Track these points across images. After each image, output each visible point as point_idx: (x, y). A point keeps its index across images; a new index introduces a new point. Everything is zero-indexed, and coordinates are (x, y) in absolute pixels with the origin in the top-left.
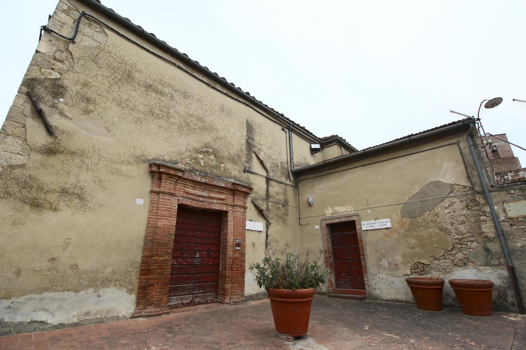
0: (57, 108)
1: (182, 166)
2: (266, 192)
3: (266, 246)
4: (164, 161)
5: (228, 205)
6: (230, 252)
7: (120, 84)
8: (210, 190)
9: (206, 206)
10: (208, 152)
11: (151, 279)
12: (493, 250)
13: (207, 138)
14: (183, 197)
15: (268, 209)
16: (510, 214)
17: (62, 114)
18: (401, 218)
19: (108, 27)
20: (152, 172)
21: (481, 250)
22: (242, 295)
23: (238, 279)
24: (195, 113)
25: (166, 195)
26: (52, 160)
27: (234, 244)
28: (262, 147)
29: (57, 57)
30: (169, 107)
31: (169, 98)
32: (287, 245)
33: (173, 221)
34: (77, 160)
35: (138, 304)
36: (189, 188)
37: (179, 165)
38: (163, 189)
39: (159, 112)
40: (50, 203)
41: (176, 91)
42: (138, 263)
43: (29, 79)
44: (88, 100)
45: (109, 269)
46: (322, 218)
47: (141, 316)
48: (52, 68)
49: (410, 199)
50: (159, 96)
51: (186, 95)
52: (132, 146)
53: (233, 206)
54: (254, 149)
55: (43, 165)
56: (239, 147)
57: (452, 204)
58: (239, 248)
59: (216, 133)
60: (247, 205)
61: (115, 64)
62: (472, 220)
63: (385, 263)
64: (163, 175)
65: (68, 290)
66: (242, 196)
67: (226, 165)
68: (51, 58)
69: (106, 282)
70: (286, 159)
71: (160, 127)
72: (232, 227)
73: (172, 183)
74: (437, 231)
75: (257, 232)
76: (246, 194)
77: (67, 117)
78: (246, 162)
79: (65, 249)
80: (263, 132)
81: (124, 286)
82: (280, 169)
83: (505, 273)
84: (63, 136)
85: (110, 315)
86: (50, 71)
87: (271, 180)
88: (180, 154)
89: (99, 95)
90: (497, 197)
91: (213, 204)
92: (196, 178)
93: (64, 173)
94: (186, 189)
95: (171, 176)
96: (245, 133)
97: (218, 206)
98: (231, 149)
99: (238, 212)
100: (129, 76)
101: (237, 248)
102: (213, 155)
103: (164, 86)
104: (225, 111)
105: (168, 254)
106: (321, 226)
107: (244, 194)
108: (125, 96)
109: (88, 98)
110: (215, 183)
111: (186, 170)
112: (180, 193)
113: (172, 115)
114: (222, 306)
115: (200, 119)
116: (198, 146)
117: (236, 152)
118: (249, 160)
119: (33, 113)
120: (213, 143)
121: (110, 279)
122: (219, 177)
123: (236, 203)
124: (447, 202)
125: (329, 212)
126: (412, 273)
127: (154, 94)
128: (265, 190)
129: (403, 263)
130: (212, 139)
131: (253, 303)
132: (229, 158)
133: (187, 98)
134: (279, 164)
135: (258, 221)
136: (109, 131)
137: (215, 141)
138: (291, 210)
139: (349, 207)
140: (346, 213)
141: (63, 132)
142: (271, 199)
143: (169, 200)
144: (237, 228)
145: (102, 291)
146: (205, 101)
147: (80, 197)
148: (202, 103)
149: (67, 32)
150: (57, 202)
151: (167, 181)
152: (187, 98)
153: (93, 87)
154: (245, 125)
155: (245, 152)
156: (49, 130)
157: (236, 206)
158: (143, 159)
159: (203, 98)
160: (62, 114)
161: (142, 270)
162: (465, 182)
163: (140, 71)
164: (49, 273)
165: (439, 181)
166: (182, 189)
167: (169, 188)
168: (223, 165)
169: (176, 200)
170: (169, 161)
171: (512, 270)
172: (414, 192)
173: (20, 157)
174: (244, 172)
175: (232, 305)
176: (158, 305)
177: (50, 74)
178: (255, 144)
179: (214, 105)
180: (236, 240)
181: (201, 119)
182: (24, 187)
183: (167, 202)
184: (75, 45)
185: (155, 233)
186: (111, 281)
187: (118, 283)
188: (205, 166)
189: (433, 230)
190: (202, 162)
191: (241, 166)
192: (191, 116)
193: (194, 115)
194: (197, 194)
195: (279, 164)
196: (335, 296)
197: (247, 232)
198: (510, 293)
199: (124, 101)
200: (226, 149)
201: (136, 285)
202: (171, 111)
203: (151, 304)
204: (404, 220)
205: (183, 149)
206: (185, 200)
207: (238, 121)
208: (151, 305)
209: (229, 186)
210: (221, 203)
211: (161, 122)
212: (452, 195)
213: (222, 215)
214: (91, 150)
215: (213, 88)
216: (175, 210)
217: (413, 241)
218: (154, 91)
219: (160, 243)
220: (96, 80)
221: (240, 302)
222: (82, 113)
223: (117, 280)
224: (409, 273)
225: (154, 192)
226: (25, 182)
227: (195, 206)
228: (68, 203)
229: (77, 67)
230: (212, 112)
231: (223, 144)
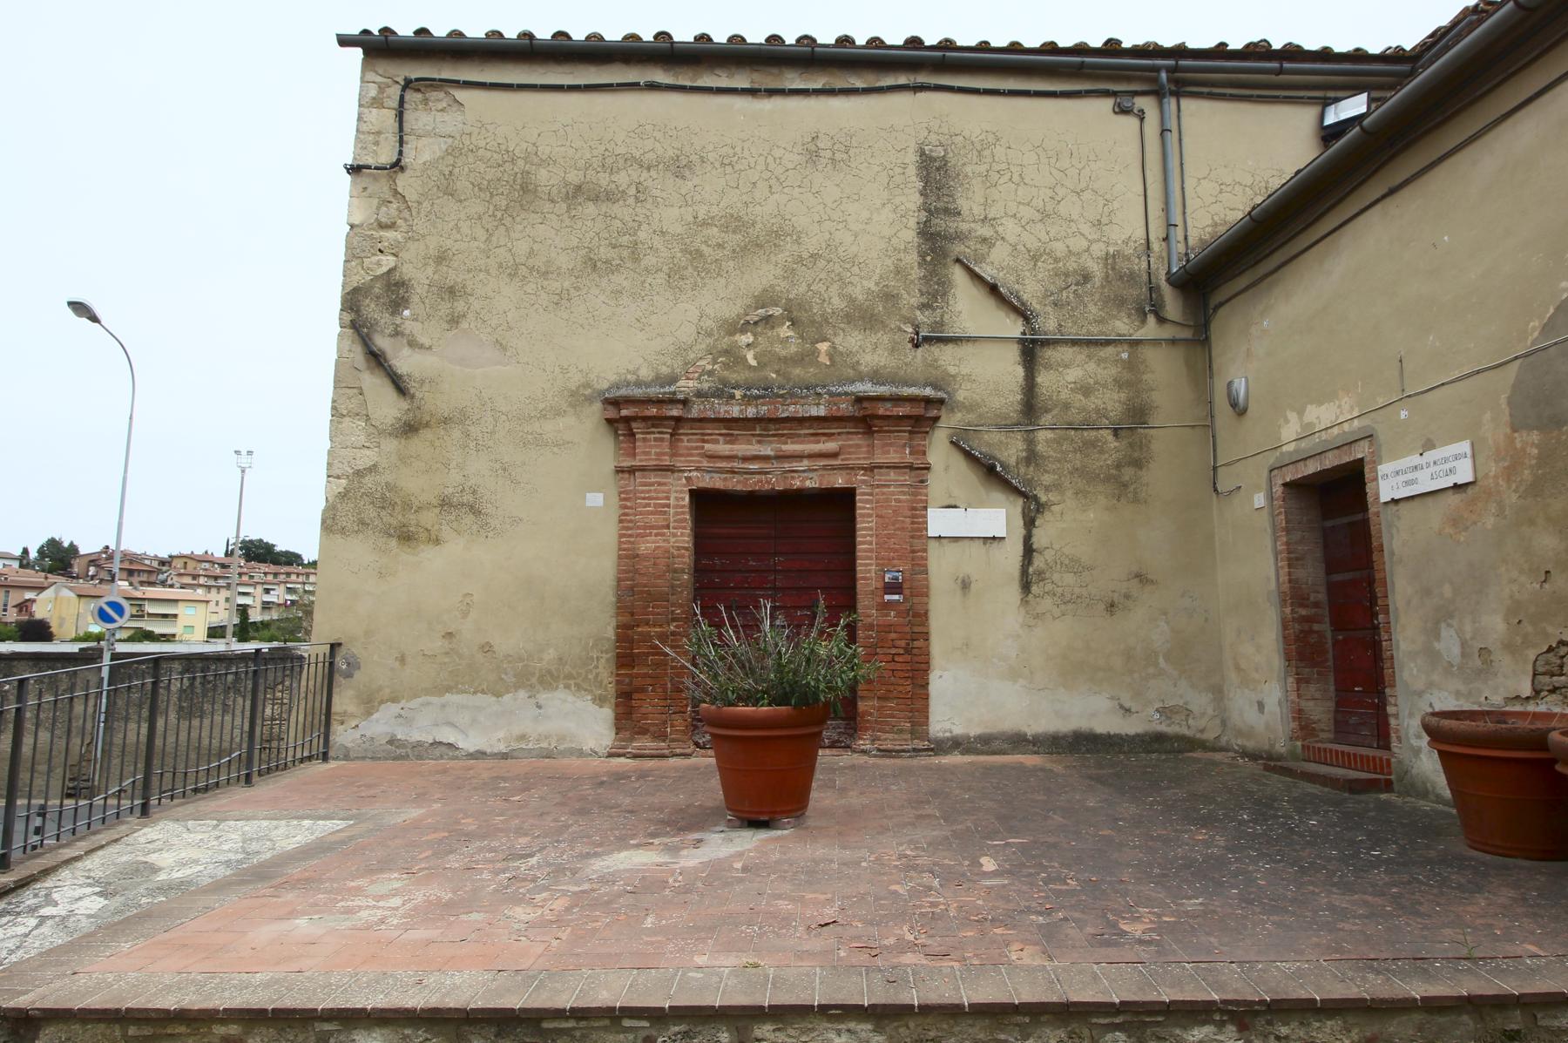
0: (403, 334)
1: (691, 383)
2: (1019, 397)
3: (1026, 586)
4: (639, 384)
5: (852, 468)
7: (508, 221)
8: (783, 435)
9: (774, 481)
10: (767, 319)
11: (638, 675)
13: (763, 275)
14: (698, 469)
15: (1032, 457)
17: (413, 344)
18: (1508, 430)
20: (610, 421)
22: (925, 736)
23: (901, 688)
24: (715, 210)
25: (652, 474)
26: (418, 444)
27: (880, 585)
28: (1000, 229)
29: (383, 220)
30: (636, 224)
31: (631, 201)
32: (1138, 576)
34: (456, 433)
35: (619, 729)
36: (717, 442)
37: (681, 383)
38: (641, 461)
40: (427, 529)
41: (649, 169)
42: (608, 639)
43: (348, 293)
45: (550, 654)
46: (1271, 459)
47: (623, 755)
48: (380, 251)
49: (1547, 329)
50: (604, 208)
51: (679, 168)
52: (557, 370)
54: (958, 249)
55: (404, 459)
56: (889, 262)
58: (896, 597)
59: (795, 247)
63: (1449, 645)
64: (634, 425)
65: (483, 692)
66: (904, 431)
67: (838, 340)
68: (374, 229)
69: (548, 680)
70: (1140, 233)
71: (618, 293)
72: (871, 536)
73: (662, 440)
75: (981, 541)
77: (421, 347)
78: (924, 307)
79: (465, 615)
80: (1004, 166)
81: (586, 690)
82: (1103, 287)
84: (424, 389)
85: (566, 746)
86: (377, 258)
87: (1046, 343)
88: (682, 349)
89: (469, 271)
91: (796, 475)
92: (726, 412)
93: (439, 465)
94: (707, 446)
96: (917, 199)
97: (816, 478)
98: (855, 280)
99: (889, 486)
100: (525, 189)
101: (887, 597)
102: (788, 323)
103: (615, 169)
104: (822, 153)
105: (674, 620)
106: (1271, 497)
107: (912, 422)
108: (522, 247)
109: (452, 287)
110: (792, 410)
112: (692, 461)
113: (646, 246)
115: (734, 223)
116: (731, 311)
117: (877, 284)
119: (368, 361)
121: (555, 674)
123: (880, 459)
126: (1537, 692)
127: (591, 209)
128: (1018, 389)
129: (1509, 647)
130: (779, 272)
131: (955, 759)
132: (847, 315)
133: (687, 173)
134: (1096, 269)
135: (981, 504)
136: (504, 348)
137: (789, 273)
139: (1346, 402)
140: (1336, 431)
141: (422, 382)
142: (1046, 419)
143: (660, 484)
144: (889, 536)
145: (543, 697)
146: (746, 152)
147: (475, 510)
148: (737, 168)
149: (386, 156)
150: (436, 527)
151: (648, 436)
152: (687, 173)
153: (455, 258)
154: (912, 171)
155: (916, 273)
156: (399, 384)
157: (881, 467)
158: (586, 393)
159: (738, 150)
160: (413, 344)
161: (618, 656)
164: (446, 660)
166: (697, 448)
167: (657, 454)
168: (823, 347)
169: (684, 481)
170: (653, 381)
173: (367, 452)
174: (917, 346)
175: (875, 756)
176: (662, 736)
177: (379, 264)
178: (964, 227)
179: (778, 153)
180: (885, 572)
181: (739, 219)
182: (383, 508)
183: (655, 490)
184: (408, 173)
185: (636, 571)
186: (559, 677)
187: (572, 682)
188: (762, 365)
191: (900, 329)
192: (705, 224)
193: (713, 218)
194: (740, 454)
195: (1096, 269)
196: (1281, 767)
197: (933, 547)
199: (523, 260)
200: (836, 286)
201: (611, 689)
203: (643, 731)
204: (1520, 439)
205: (687, 334)
206: (707, 477)
207: (880, 168)
208: (644, 734)
209: (845, 408)
210: (825, 468)
211: (618, 279)
213: (843, 500)
214: (477, 404)
215: (771, 92)
216: (683, 506)
219: (649, 593)
220: (459, 237)
221: (903, 751)
222: (446, 326)
223: (569, 676)
224: (1526, 690)
225: (623, 472)
226: (383, 498)
227: (739, 488)
228: (455, 525)
229: (420, 225)
230: (773, 182)
231: (823, 275)
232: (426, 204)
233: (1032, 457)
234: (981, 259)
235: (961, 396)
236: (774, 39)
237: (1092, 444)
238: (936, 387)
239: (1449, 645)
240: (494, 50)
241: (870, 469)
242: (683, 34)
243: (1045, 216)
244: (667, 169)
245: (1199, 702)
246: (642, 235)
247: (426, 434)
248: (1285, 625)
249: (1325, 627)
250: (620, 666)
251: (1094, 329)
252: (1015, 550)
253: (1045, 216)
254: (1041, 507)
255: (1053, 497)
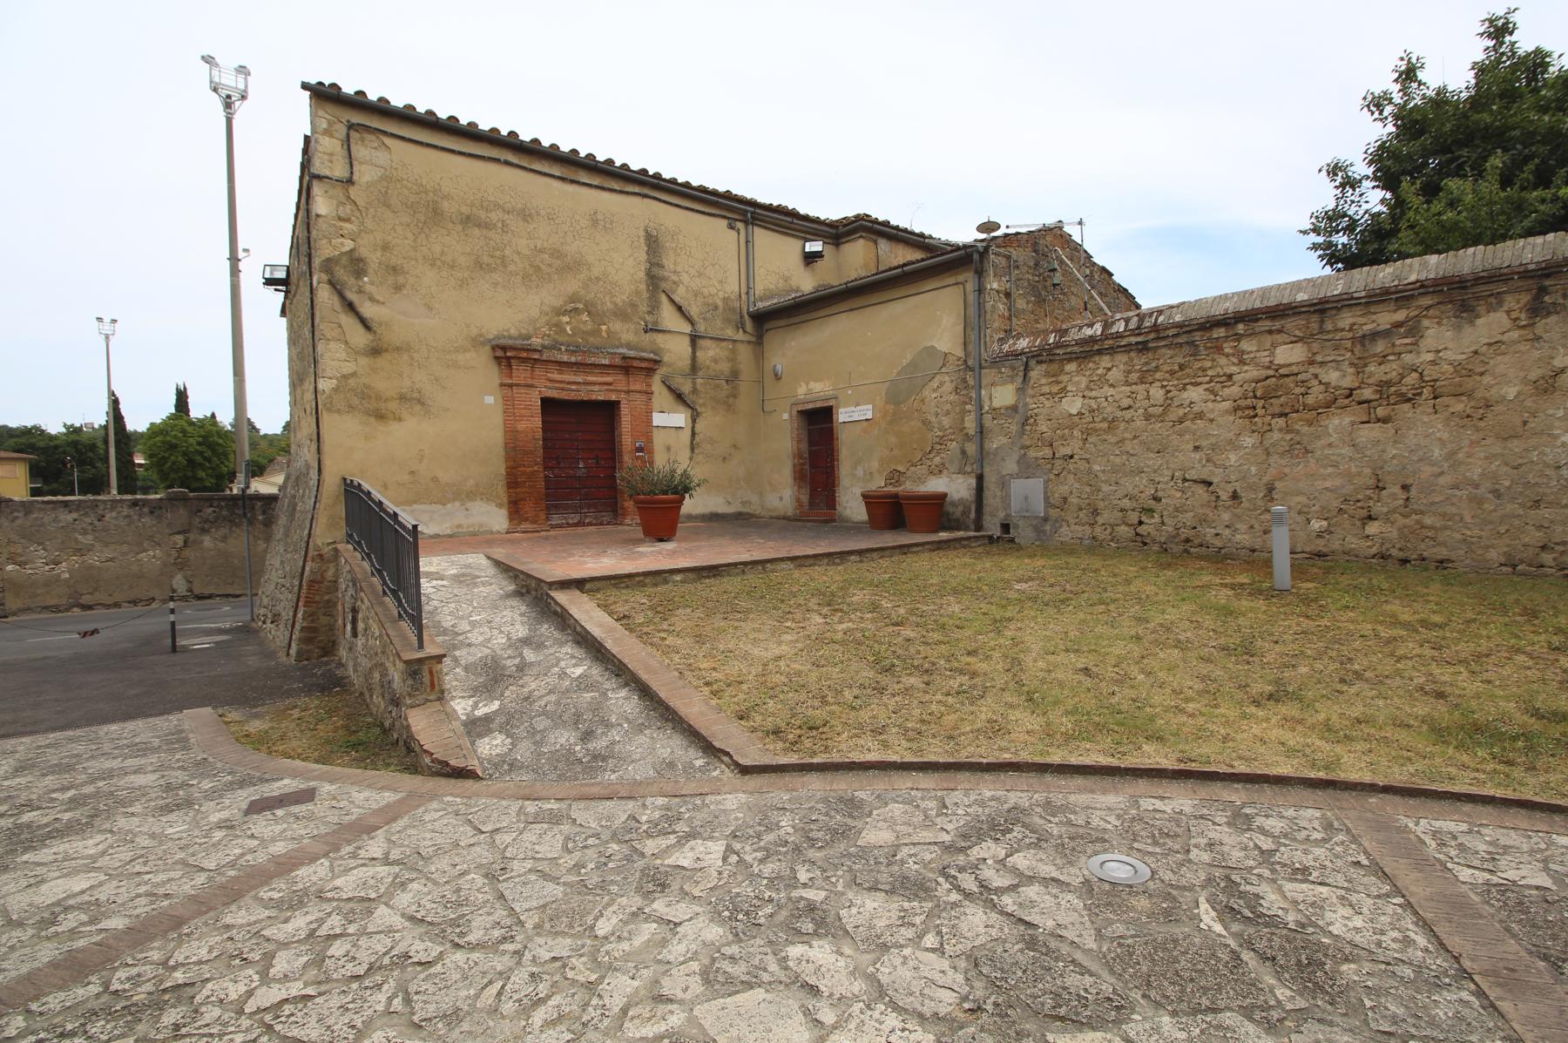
3: (692, 450)
4: (510, 337)
6: (627, 459)
7: (426, 230)
9: (583, 396)
12: (969, 453)
13: (572, 285)
15: (695, 391)
16: (996, 404)
17: (372, 299)
19: (385, 133)
20: (496, 358)
21: (959, 452)
26: (381, 361)
33: (537, 422)
34: (405, 357)
37: (534, 339)
39: (491, 260)
44: (394, 269)
45: (471, 482)
46: (793, 400)
49: (899, 373)
50: (485, 232)
51: (526, 215)
53: (628, 392)
54: (663, 285)
57: (942, 384)
60: (654, 388)
61: (413, 198)
62: (958, 409)
63: (860, 472)
71: (496, 284)
74: (920, 424)
76: (650, 372)
77: (378, 302)
78: (649, 313)
79: (421, 461)
83: (973, 482)
90: (988, 375)
95: (525, 360)
96: (644, 256)
100: (435, 211)
106: (791, 416)
108: (437, 248)
110: (592, 360)
111: (544, 347)
114: (620, 527)
115: (557, 253)
116: (558, 303)
118: (654, 307)
119: (343, 306)
120: (583, 292)
122: (599, 349)
124: (935, 383)
125: (802, 391)
127: (476, 231)
129: (879, 472)
134: (720, 304)
136: (430, 308)
137: (586, 286)
138: (744, 386)
139: (827, 383)
141: (381, 324)
142: (700, 373)
147: (423, 404)
154: (642, 240)
155: (645, 295)
160: (372, 299)
162: (960, 353)
163: (447, 197)
165: (933, 347)
171: (980, 478)
172: (905, 362)
177: (342, 244)
179: (578, 218)
181: (558, 251)
184: (356, 186)
188: (574, 334)
189: (916, 424)
190: (568, 329)
192: (541, 251)
195: (720, 304)
197: (655, 430)
198: (973, 508)
201: (505, 500)
202: (507, 252)
204: (888, 407)
205: (535, 313)
209: (617, 361)
211: (496, 276)
212: (944, 370)
213: (610, 409)
215: (573, 182)
217: (893, 440)
218: (475, 225)
223: (482, 494)
229: (369, 223)
232: (372, 210)
233: (695, 391)
234: (674, 293)
235: (666, 359)
236: (574, 151)
237: (717, 386)
238: (655, 354)
239: (860, 472)
240: (407, 116)
241: (628, 392)
242: (525, 136)
243: (700, 275)
244: (518, 215)
245: (754, 499)
246: (507, 252)
247: (386, 356)
248: (794, 466)
249: (807, 467)
250: (509, 488)
251: (720, 333)
252: (688, 433)
253: (700, 275)
254: (698, 414)
255: (703, 409)
